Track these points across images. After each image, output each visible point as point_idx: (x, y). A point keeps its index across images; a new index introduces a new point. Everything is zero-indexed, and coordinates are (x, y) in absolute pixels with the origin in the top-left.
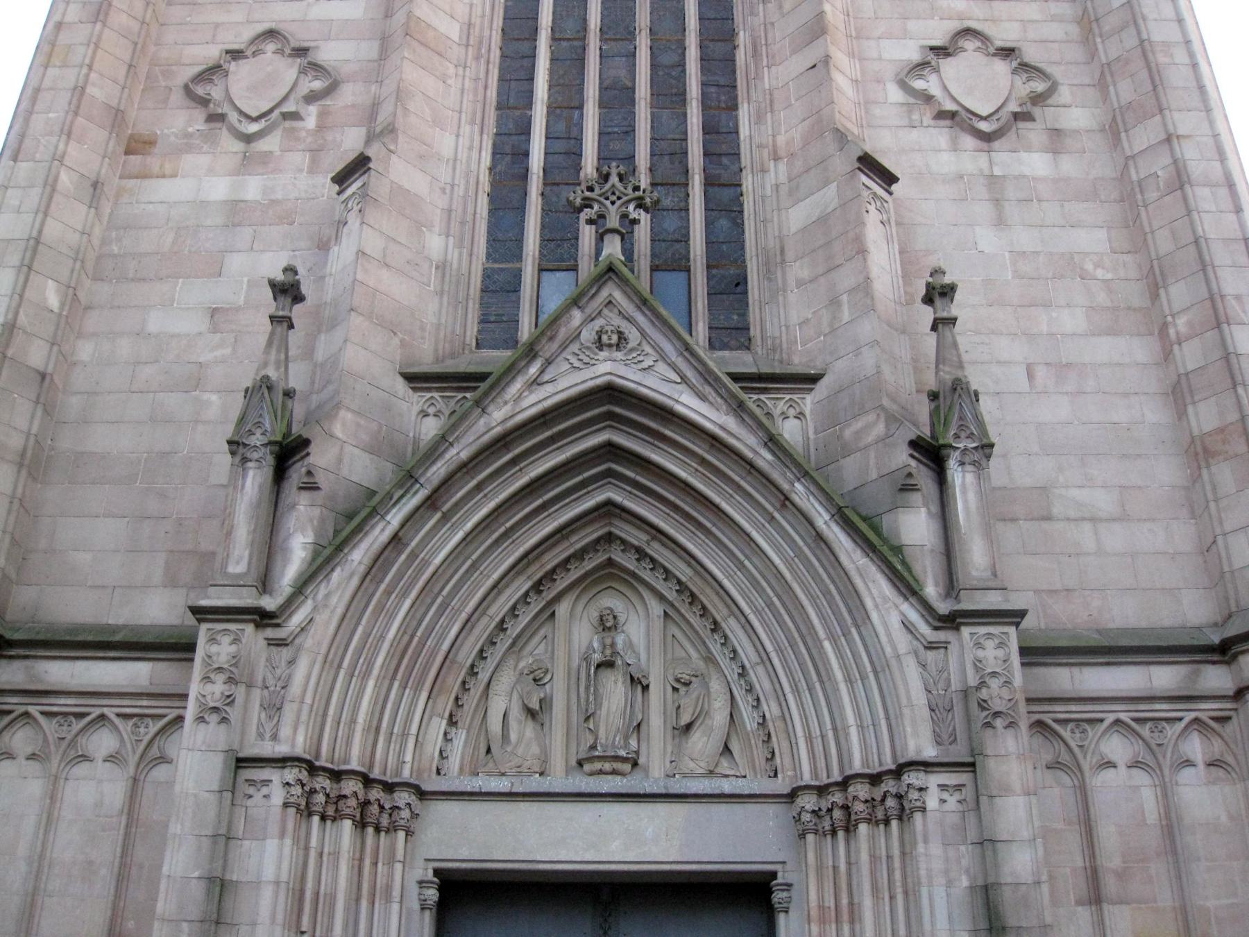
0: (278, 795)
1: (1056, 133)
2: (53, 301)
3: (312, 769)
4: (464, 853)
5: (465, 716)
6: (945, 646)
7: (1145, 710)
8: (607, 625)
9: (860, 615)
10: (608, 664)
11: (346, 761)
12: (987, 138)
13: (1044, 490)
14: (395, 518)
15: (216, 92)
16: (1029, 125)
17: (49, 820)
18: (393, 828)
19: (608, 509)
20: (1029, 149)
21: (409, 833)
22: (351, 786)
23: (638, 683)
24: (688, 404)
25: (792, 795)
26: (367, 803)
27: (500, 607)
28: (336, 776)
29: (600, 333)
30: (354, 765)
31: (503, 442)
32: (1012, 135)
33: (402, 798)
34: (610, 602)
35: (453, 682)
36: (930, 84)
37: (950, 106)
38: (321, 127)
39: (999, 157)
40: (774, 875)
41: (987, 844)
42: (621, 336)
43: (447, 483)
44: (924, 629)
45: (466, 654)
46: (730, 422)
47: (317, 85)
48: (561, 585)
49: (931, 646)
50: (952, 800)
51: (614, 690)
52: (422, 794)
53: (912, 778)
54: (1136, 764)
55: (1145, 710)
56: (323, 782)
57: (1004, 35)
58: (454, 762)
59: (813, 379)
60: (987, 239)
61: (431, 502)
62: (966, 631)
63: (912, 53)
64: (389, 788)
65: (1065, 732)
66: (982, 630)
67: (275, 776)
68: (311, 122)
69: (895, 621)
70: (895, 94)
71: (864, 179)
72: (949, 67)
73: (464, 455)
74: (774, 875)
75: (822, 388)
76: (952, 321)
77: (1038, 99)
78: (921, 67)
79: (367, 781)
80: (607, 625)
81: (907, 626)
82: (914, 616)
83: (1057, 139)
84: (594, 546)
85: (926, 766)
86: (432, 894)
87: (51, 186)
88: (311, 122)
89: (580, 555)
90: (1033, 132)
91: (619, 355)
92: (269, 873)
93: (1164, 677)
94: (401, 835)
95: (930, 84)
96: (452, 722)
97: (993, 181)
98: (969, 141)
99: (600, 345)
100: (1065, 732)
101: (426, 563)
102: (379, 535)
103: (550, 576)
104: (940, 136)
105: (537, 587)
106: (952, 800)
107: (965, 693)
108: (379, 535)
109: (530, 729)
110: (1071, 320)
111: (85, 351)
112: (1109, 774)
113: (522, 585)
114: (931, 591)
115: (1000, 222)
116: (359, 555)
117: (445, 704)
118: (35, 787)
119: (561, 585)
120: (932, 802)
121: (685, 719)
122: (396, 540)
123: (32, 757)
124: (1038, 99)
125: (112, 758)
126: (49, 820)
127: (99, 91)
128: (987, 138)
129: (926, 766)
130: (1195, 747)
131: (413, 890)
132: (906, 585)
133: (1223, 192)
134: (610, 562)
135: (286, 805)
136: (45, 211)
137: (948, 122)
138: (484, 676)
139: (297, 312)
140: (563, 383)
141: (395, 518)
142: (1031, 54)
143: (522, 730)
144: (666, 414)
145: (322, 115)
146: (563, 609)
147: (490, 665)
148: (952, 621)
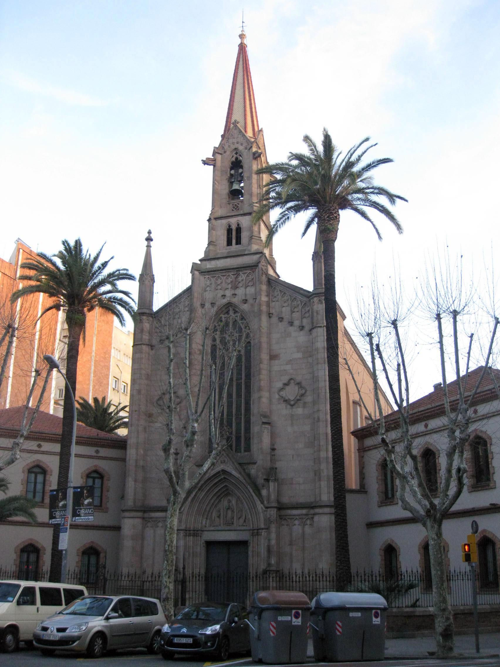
0: (182, 535)
1: (305, 403)
2: (142, 452)
3: (186, 530)
4: (208, 538)
5: (209, 517)
6: (267, 511)
7: (301, 517)
8: (229, 501)
9: (255, 507)
10: (228, 509)
11: (191, 528)
12: (292, 405)
13: (292, 479)
14: (194, 493)
15: (161, 402)
16: (300, 401)
17: (154, 536)
18: (198, 536)
19: (226, 486)
20: (299, 407)
21: (201, 537)
22: (191, 532)
23: (233, 511)
24: (234, 473)
25: (250, 530)
26: (194, 533)
27: (212, 501)
28: (190, 530)
29: (221, 461)
30: (192, 529)
31: (209, 479)
32: (296, 405)
33: (199, 532)
34: (230, 498)
35: (206, 513)
36: (283, 393)
37: (287, 398)
38: (180, 410)
39: (294, 410)
40: (248, 541)
41: (269, 540)
42: (224, 461)
43: (201, 486)
44: (264, 508)
45: (208, 510)
46: (239, 476)
47: (179, 400)
48: (221, 497)
49: (265, 511)
50: (266, 534)
51: (230, 512)
52: (203, 531)
53: (260, 531)
54: (299, 525)
55: (301, 517)
56: (188, 532)
57: (299, 378)
58: (208, 525)
59: (255, 463)
60: (289, 429)
61: (199, 490)
62: (269, 509)
63: (279, 385)
64: (197, 531)
65: (288, 520)
66: (271, 509)
67: (182, 532)
68: (178, 410)
69: (260, 508)
70: (277, 396)
71: (263, 426)
72: (288, 388)
73: (203, 482)
74: (248, 541)
75: (257, 464)
76: (275, 455)
77: (302, 395)
78: (281, 389)
79: (194, 531)
80: (229, 501)
81: (262, 508)
82: (263, 506)
83: (305, 405)
84: (226, 490)
85: (263, 529)
86: (204, 544)
87: (138, 432)
88: (178, 410)
89: (224, 492)
90: (301, 403)
91: (224, 464)
92: (182, 544)
93: (304, 511)
94: (199, 537)
95: (283, 393)
96: (207, 519)
97: (292, 416)
98: (289, 406)
99: (221, 463)
100: (288, 520)
101: (200, 498)
102: (192, 495)
103: (219, 496)
104: (283, 405)
105: (218, 497)
106: (266, 534)
107: (269, 518)
108: (192, 495)
109: (218, 519)
110: (301, 446)
111: (149, 459)
112: (295, 526)
113: (215, 497)
114: (265, 502)
115: (292, 425)
116: (190, 499)
117: (205, 516)
118: (152, 531)
119: (221, 497)
120: (263, 534)
121: (239, 517)
122: (195, 495)
123: (151, 527)
124: (302, 395)
125: (162, 527)
126: (154, 536)
127: (143, 408)
128: (292, 405)
129: (263, 529)
130: (308, 522)
131: (202, 544)
132: (262, 503)
133: (325, 423)
134: (228, 492)
135: (183, 536)
136: (138, 437)
137: (285, 402)
138: (211, 512)
139: (179, 456)
140: (216, 470)
141: (194, 493)
142: (304, 384)
143: (218, 519)
144: (231, 474)
145: (180, 407)
146: (222, 499)
147: (212, 509)
148: (267, 508)
